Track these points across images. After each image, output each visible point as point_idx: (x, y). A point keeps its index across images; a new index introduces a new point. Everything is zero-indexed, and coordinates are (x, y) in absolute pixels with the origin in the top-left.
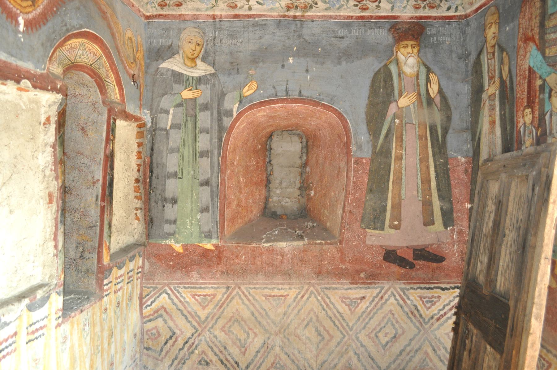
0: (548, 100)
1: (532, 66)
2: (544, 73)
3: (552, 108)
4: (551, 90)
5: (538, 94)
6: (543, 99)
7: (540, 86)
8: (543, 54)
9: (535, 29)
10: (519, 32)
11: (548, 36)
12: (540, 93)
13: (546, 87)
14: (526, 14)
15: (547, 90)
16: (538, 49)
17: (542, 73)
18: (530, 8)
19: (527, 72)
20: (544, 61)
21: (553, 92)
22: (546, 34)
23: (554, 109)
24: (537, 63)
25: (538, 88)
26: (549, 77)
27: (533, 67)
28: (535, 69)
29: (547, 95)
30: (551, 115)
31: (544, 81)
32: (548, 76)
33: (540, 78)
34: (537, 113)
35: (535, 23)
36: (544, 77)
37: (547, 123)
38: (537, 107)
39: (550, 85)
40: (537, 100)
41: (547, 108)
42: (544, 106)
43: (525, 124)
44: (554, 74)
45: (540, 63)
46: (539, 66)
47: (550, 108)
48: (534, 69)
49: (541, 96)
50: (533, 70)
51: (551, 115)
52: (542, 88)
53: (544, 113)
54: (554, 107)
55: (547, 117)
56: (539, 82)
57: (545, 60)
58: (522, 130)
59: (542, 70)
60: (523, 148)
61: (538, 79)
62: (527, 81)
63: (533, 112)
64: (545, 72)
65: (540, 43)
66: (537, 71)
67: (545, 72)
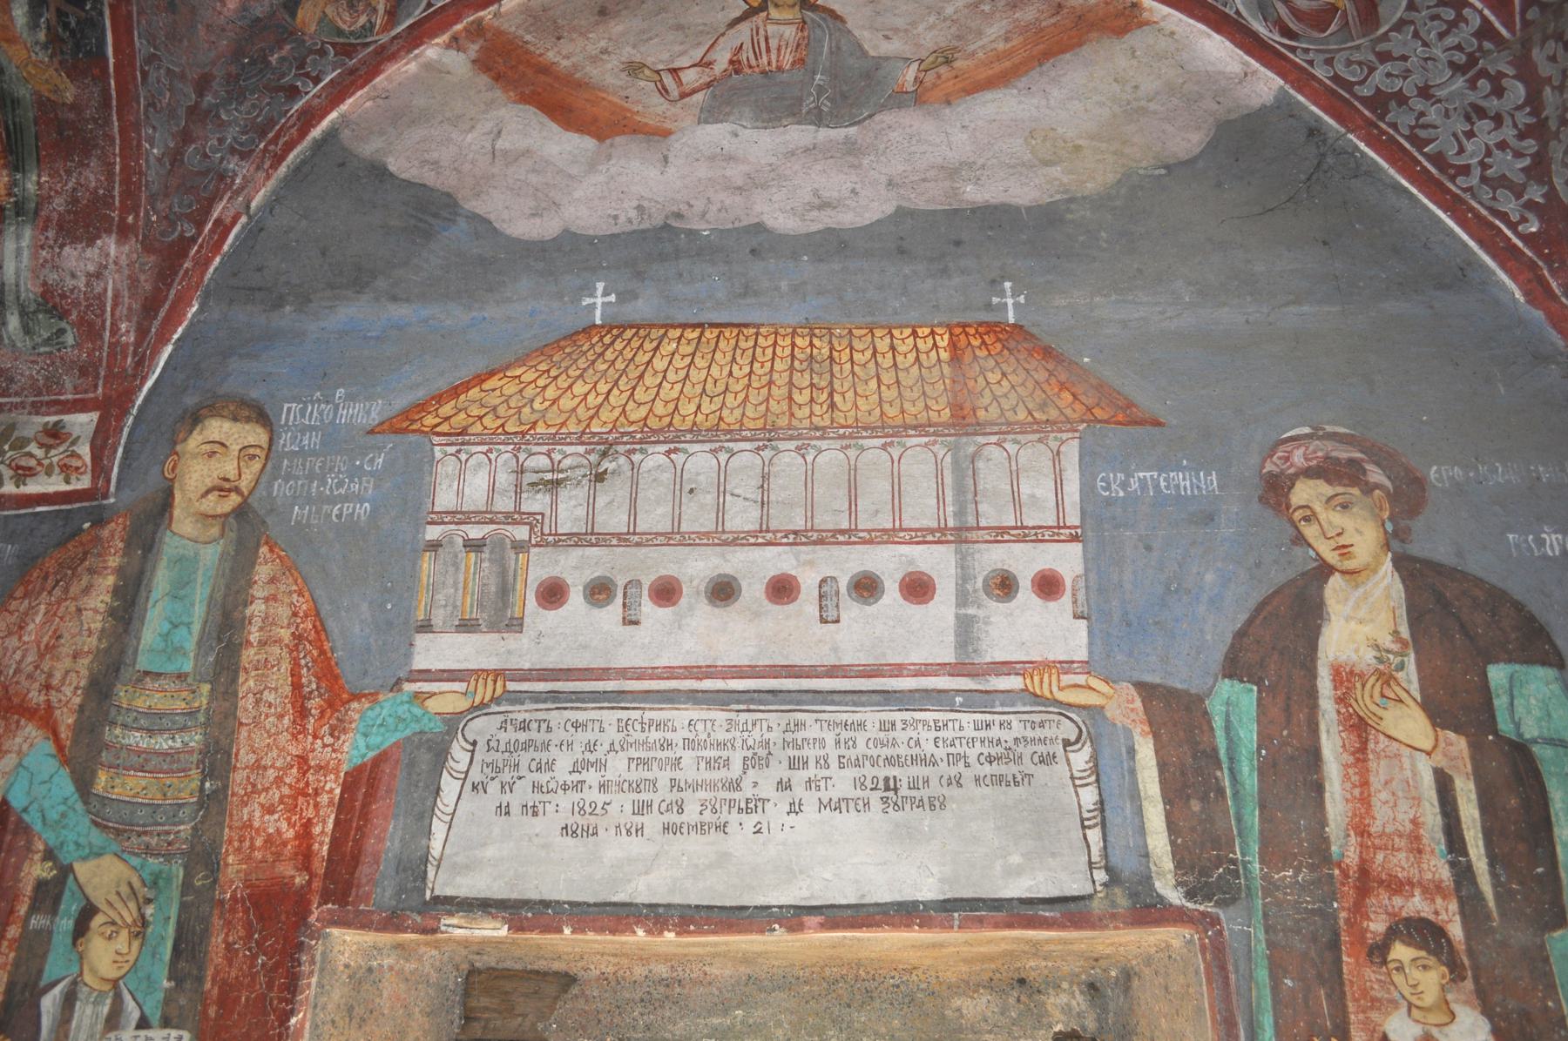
0: (69, 940)
2: (72, 847)
3: (81, 974)
4: (88, 912)
5: (23, 909)
6: (46, 936)
7: (41, 885)
8: (84, 785)
9: (68, 691)
11: (118, 731)
12: (34, 909)
13: (67, 895)
14: (31, 627)
15: (70, 907)
16: (63, 755)
17: (62, 844)
18: (50, 615)
20: (79, 806)
21: (98, 920)
22: (113, 723)
23: (87, 978)
24: (46, 804)
25: (28, 889)
26: (92, 863)
27: (25, 810)
29: (66, 924)
30: (69, 1000)
31: (66, 871)
32: (84, 859)
33: (49, 855)
35: (67, 672)
36: (65, 857)
37: (46, 1022)
39: (89, 891)
40: (13, 931)
41: (56, 965)
42: (44, 956)
44: (115, 859)
45: (62, 808)
46: (53, 815)
47: (75, 970)
48: (25, 817)
49: (37, 922)
50: (20, 821)
51: (69, 1000)
52: (48, 895)
53: (36, 984)
54: (93, 971)
55: (49, 1004)
56: (37, 870)
57: (86, 803)
59: (64, 832)
61: (37, 857)
64: (77, 844)
65: (75, 741)
66: (38, 826)
67: (77, 844)
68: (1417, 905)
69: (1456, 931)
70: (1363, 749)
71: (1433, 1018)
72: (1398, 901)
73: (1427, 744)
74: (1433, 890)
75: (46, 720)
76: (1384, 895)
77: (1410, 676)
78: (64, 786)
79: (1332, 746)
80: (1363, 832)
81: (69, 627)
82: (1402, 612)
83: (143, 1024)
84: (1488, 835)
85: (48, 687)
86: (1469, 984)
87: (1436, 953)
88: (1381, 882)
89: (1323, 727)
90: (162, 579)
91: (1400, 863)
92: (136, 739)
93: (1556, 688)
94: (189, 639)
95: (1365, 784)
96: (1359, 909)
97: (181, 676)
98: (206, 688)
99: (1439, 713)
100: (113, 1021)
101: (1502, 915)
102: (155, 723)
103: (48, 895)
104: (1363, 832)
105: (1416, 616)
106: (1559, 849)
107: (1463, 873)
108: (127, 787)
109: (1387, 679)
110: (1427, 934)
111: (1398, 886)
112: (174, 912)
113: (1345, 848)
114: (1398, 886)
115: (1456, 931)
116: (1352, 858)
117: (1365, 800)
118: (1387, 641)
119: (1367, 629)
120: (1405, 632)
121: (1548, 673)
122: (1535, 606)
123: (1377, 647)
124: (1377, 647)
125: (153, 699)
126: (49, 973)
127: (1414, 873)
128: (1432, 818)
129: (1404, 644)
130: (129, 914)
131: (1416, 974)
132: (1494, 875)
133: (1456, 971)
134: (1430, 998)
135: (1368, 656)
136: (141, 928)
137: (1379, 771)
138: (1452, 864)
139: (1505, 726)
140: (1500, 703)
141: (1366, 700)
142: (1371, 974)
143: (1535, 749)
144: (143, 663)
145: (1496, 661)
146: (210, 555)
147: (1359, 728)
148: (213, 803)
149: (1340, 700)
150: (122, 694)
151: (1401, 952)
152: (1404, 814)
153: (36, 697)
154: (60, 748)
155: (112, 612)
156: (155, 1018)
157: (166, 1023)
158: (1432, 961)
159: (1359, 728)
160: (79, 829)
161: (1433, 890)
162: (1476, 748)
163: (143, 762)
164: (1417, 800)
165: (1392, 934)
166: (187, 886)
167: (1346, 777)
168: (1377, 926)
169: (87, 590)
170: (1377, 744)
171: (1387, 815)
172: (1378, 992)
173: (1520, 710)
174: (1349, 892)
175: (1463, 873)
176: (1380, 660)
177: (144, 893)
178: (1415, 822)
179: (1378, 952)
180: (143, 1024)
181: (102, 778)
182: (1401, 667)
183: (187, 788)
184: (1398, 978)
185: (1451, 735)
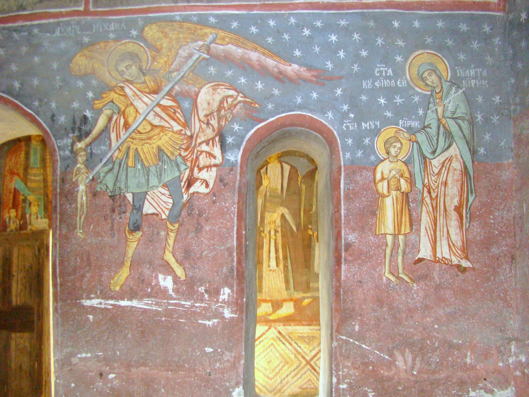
1: (17, 187)
4: (30, 204)
8: (26, 185)
10: (5, 167)
15: (28, 203)
16: (23, 180)
18: (15, 159)
19: (13, 191)
21: (32, 205)
28: (19, 190)
29: (27, 205)
30: (30, 215)
31: (26, 198)
33: (23, 195)
34: (20, 213)
36: (26, 195)
38: (20, 210)
40: (20, 206)
41: (27, 211)
43: (10, 217)
51: (30, 215)
55: (28, 216)
56: (22, 197)
58: (7, 220)
60: (8, 230)
62: (12, 195)
63: (17, 211)
75: (18, 175)
78: (23, 185)
81: (19, 160)
83: (41, 218)
85: (17, 170)
90: (32, 152)
92: (33, 178)
94: (38, 161)
97: (38, 168)
98: (42, 170)
100: (37, 218)
102: (35, 175)
103: (24, 201)
108: (33, 185)
112: (43, 203)
125: (34, 171)
126: (27, 211)
130: (36, 203)
136: (38, 205)
144: (31, 166)
146: (39, 148)
148: (45, 187)
150: (29, 171)
153: (16, 171)
154: (21, 179)
155: (25, 158)
156: (43, 217)
157: (45, 218)
160: (27, 192)
163: (34, 181)
166: (44, 199)
169: (20, 154)
177: (39, 200)
180: (41, 218)
181: (29, 184)
183: (42, 185)
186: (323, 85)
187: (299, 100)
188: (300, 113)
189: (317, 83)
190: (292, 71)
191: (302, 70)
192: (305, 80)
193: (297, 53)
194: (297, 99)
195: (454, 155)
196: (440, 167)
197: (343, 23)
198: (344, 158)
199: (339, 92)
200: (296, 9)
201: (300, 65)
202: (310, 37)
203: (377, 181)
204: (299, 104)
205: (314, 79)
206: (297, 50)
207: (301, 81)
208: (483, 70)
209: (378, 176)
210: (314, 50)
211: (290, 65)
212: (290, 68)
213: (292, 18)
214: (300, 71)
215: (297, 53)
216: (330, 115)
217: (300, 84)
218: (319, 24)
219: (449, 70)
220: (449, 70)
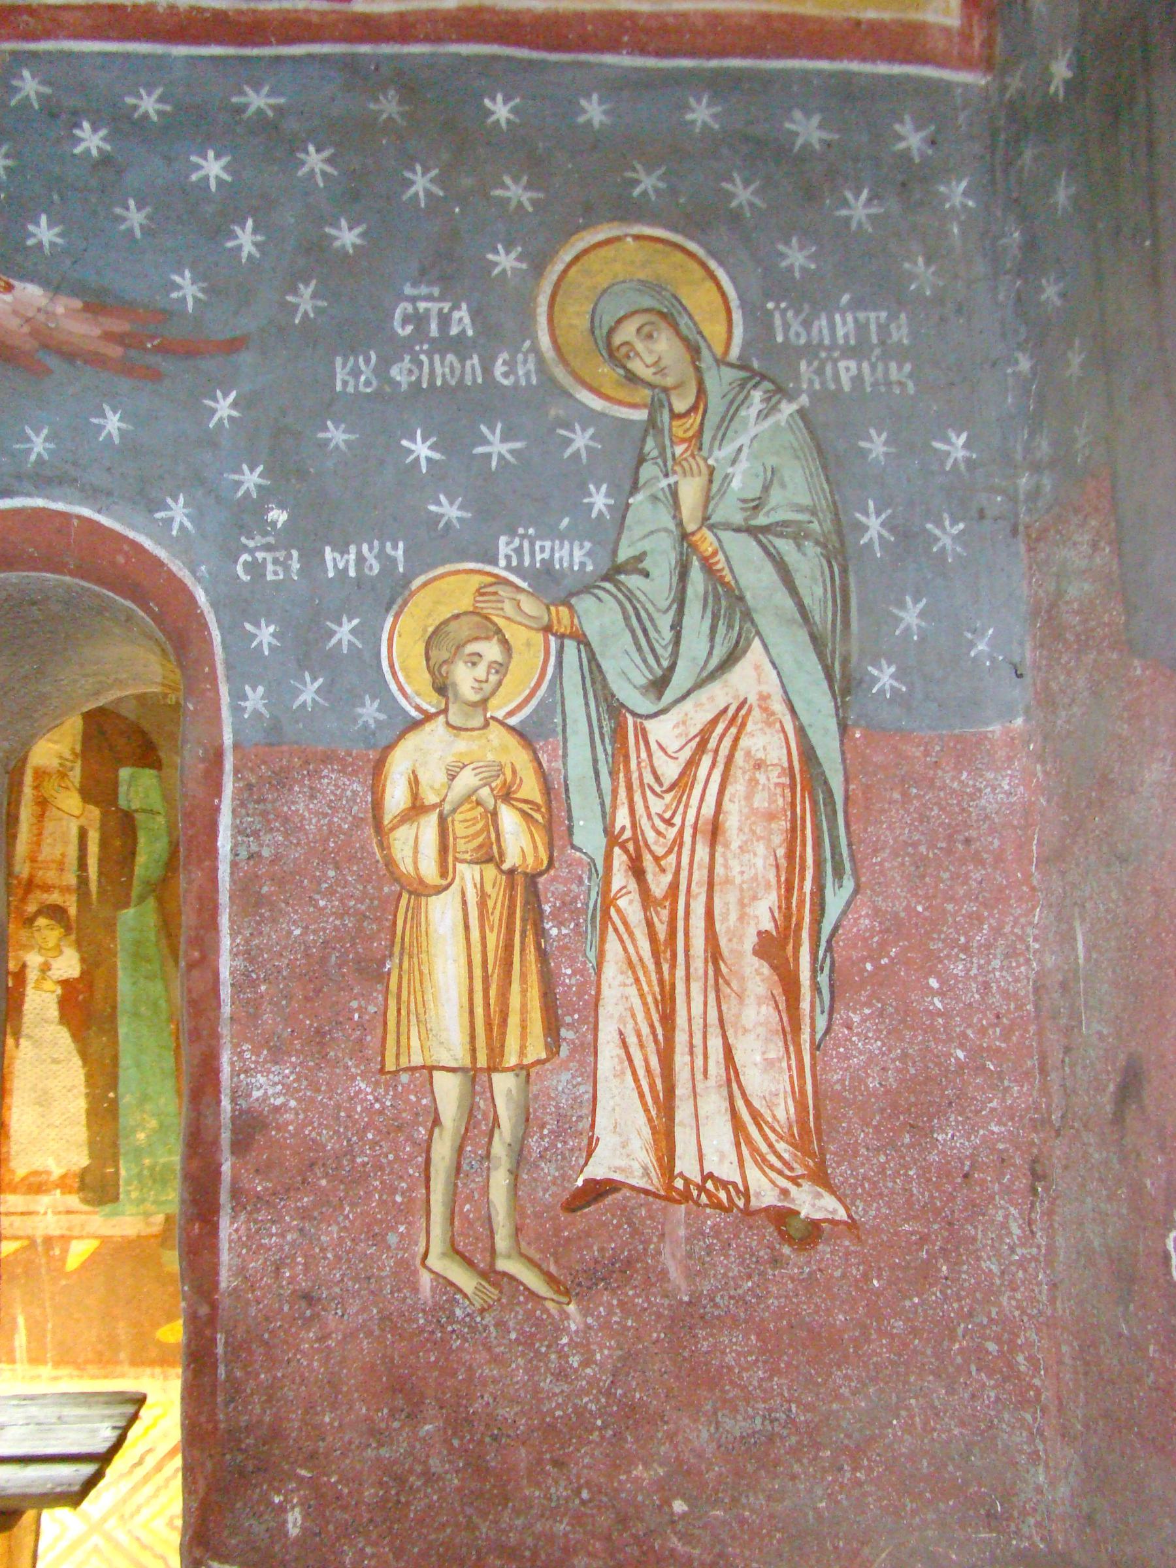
68: (55, 898)
69: (73, 911)
70: (42, 815)
71: (50, 954)
72: (45, 896)
73: (77, 812)
74: (65, 890)
76: (38, 892)
77: (76, 775)
79: (26, 813)
80: (33, 860)
82: (79, 738)
84: (101, 861)
86: (73, 937)
87: (59, 922)
88: (38, 886)
89: (23, 803)
91: (51, 876)
93: (155, 781)
95: (40, 834)
96: (24, 900)
99: (87, 795)
101: (99, 901)
104: (33, 860)
105: (87, 738)
106: (137, 868)
107: (83, 881)
109: (63, 775)
110: (56, 913)
111: (47, 888)
113: (23, 869)
114: (47, 888)
115: (73, 911)
116: (25, 874)
117: (38, 844)
118: (67, 754)
119: (56, 747)
120: (78, 748)
121: (153, 772)
122: (155, 737)
123: (61, 757)
124: (61, 757)
127: (57, 882)
128: (73, 852)
129: (76, 755)
131: (47, 932)
132: (99, 882)
133: (68, 929)
134: (51, 944)
135: (55, 763)
137: (49, 826)
138: (79, 877)
139: (122, 803)
140: (122, 789)
141: (50, 788)
142: (24, 934)
143: (136, 815)
145: (126, 765)
147: (43, 804)
149: (36, 788)
151: (42, 921)
152: (58, 853)
158: (57, 926)
159: (43, 804)
161: (65, 890)
162: (105, 814)
164: (66, 843)
165: (39, 913)
167: (30, 831)
168: (31, 908)
170: (52, 812)
171: (48, 852)
172: (24, 940)
173: (132, 794)
174: (20, 892)
175: (83, 881)
176: (61, 765)
178: (63, 855)
179: (29, 921)
182: (72, 769)
184: (36, 934)
185: (92, 807)
186: (156, 376)
187: (39, 445)
188: (40, 502)
189: (128, 369)
190: (15, 313)
191: (60, 310)
192: (70, 355)
193: (44, 232)
194: (29, 440)
195: (752, 699)
196: (686, 754)
197: (257, 101)
198: (237, 710)
199: (224, 407)
200: (48, 35)
201: (55, 287)
202: (105, 160)
203: (387, 820)
204: (40, 461)
205: (114, 351)
206: (44, 219)
207: (53, 362)
208: (893, 317)
209: (396, 797)
210: (124, 219)
211: (9, 288)
212: (8, 298)
213: (26, 74)
214: (50, 315)
215: (44, 232)
216: (178, 512)
217: (49, 371)
218: (149, 104)
219: (737, 316)
220: (737, 316)
